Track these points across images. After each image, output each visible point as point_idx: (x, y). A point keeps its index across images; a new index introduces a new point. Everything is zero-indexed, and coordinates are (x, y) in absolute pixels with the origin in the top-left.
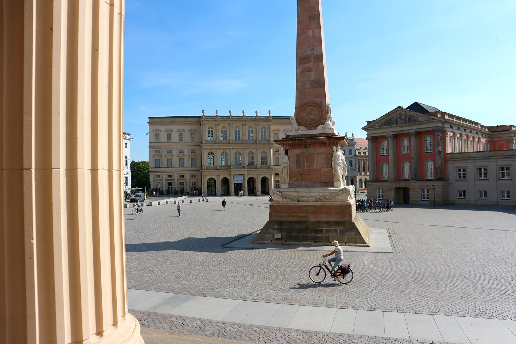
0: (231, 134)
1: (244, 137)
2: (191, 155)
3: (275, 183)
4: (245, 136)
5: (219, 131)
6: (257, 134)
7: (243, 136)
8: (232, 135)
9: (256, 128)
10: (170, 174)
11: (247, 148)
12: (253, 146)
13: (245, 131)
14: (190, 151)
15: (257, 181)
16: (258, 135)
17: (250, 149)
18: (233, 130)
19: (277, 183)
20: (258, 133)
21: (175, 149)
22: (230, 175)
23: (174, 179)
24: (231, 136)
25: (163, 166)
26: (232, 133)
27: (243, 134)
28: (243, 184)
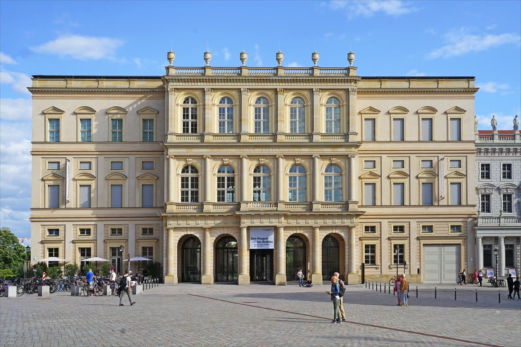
3: (364, 254)
15: (311, 244)
19: (370, 254)
22: (240, 230)
28: (275, 251)
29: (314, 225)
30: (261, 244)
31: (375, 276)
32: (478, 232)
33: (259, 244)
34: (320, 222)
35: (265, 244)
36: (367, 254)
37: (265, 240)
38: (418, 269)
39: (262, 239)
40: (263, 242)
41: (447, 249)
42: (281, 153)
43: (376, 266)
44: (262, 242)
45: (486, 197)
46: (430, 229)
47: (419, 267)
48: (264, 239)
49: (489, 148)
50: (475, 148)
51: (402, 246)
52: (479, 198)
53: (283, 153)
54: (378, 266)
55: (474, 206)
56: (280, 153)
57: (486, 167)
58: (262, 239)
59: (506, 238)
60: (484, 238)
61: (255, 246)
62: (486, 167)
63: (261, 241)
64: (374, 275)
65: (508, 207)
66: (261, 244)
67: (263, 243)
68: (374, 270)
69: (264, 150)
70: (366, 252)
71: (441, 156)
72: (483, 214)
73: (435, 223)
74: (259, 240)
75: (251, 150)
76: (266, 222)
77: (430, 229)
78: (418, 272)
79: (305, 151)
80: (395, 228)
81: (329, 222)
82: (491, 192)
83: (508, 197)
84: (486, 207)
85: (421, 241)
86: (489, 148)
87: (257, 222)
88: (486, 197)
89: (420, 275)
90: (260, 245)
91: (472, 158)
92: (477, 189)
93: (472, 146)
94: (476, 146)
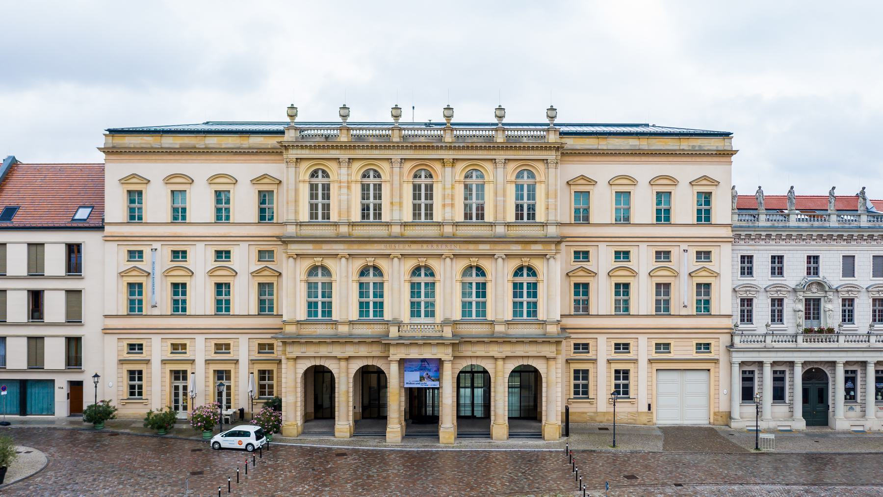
0: (396, 199)
1: (448, 209)
2: (258, 271)
4: (452, 205)
5: (349, 188)
6: (500, 198)
7: (444, 206)
8: (401, 204)
9: (495, 177)
10: (178, 339)
11: (457, 252)
12: (481, 247)
13: (453, 187)
14: (255, 255)
16: (504, 201)
18: (405, 185)
20: (504, 195)
21: (200, 246)
23: (192, 358)
24: (396, 208)
25: (156, 312)
26: (401, 197)
27: (444, 198)
29: (496, 355)
31: (588, 414)
32: (734, 355)
34: (507, 350)
36: (577, 382)
38: (649, 405)
41: (690, 376)
42: (450, 251)
43: (589, 400)
45: (747, 303)
46: (667, 346)
49: (752, 233)
50: (731, 234)
51: (626, 372)
52: (737, 304)
53: (452, 251)
54: (591, 400)
55: (730, 316)
56: (447, 251)
57: (747, 260)
59: (774, 363)
60: (743, 363)
62: (747, 260)
64: (586, 413)
65: (777, 316)
68: (587, 405)
69: (425, 246)
70: (575, 379)
71: (684, 246)
72: (742, 327)
73: (674, 339)
75: (407, 246)
76: (428, 353)
77: (664, 347)
78: (649, 409)
79: (484, 248)
80: (617, 346)
81: (520, 350)
82: (755, 295)
83: (777, 303)
84: (747, 316)
85: (654, 365)
86: (752, 233)
87: (414, 353)
88: (747, 303)
89: (652, 413)
91: (727, 248)
92: (734, 290)
93: (727, 232)
94: (732, 231)
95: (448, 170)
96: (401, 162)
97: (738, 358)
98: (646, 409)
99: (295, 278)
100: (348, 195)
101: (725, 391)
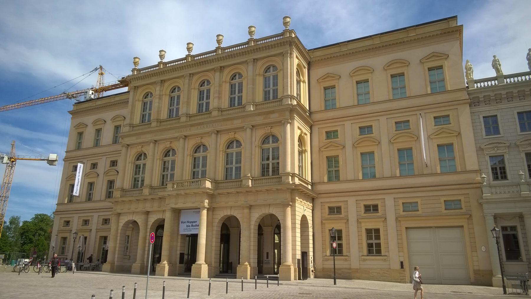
17: (228, 131)
30: (190, 228)
33: (188, 228)
35: (194, 228)
37: (194, 224)
39: (191, 222)
40: (192, 226)
44: (191, 226)
47: (402, 260)
48: (193, 222)
50: (467, 97)
58: (191, 222)
61: (184, 231)
63: (190, 224)
66: (190, 228)
67: (192, 228)
74: (188, 224)
80: (367, 208)
82: (505, 151)
89: (404, 271)
90: (189, 230)
95: (218, 74)
96: (190, 76)
97: (490, 210)
98: (398, 266)
99: (126, 160)
100: (159, 103)
101: (483, 248)
